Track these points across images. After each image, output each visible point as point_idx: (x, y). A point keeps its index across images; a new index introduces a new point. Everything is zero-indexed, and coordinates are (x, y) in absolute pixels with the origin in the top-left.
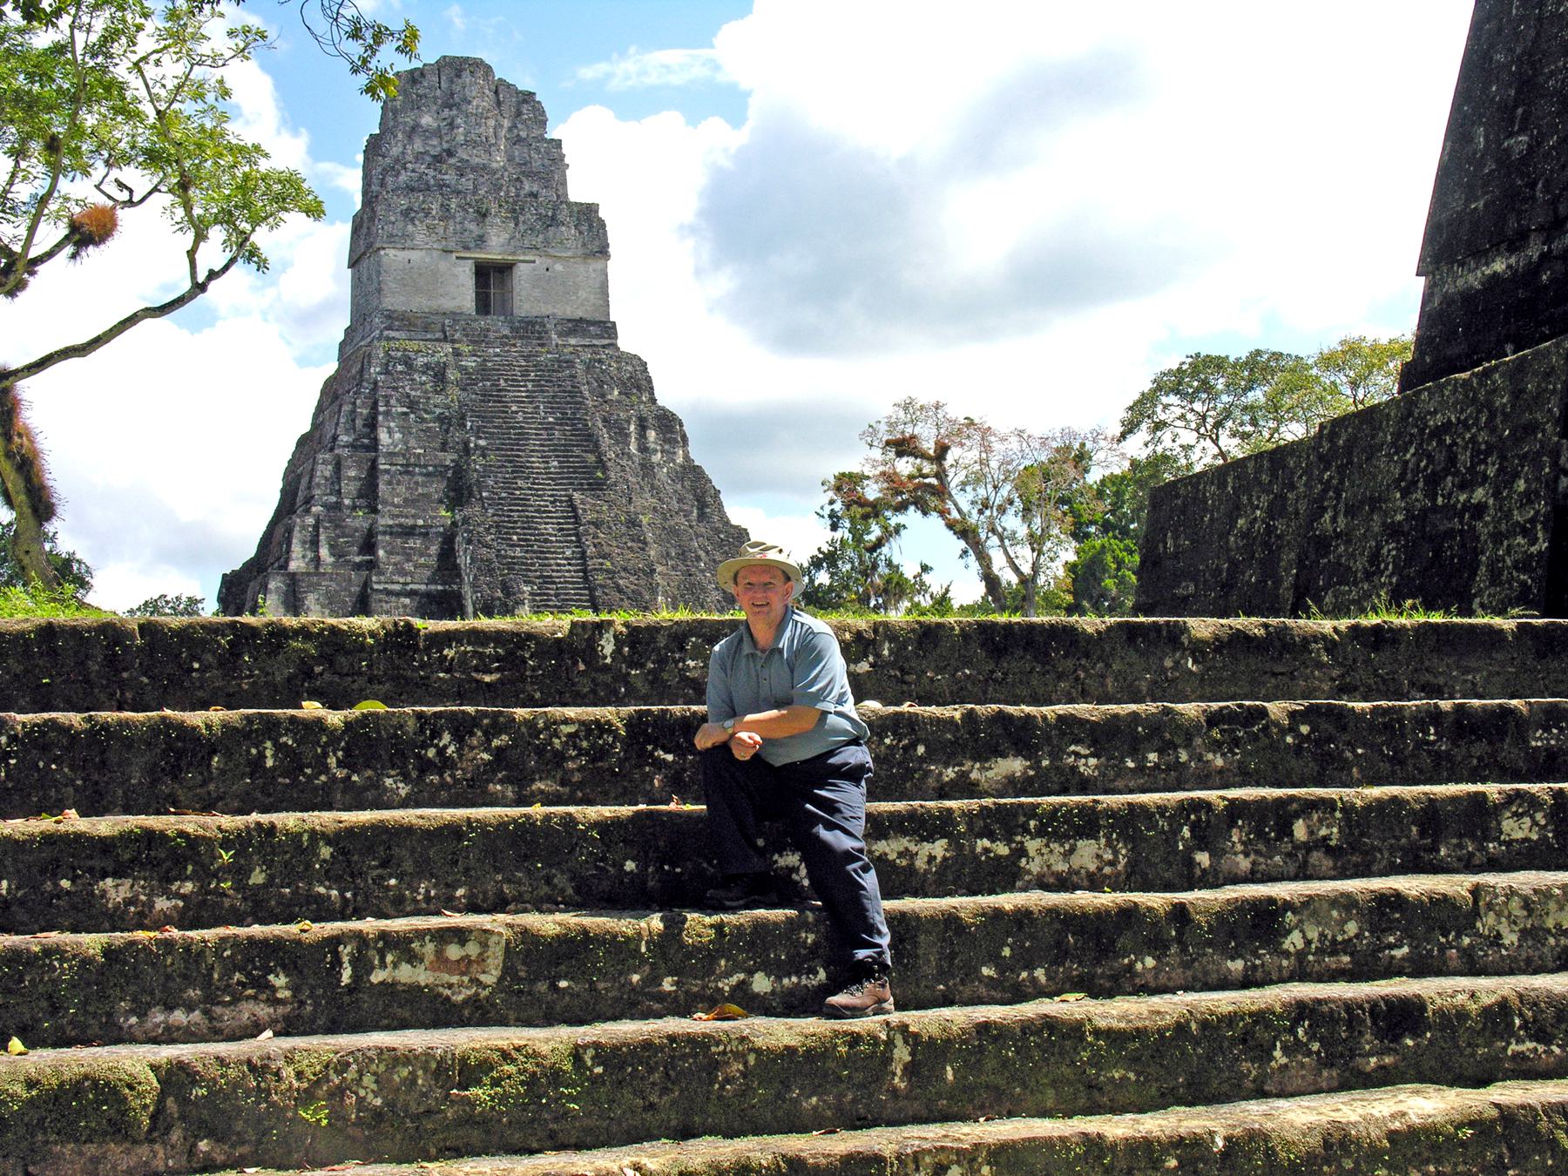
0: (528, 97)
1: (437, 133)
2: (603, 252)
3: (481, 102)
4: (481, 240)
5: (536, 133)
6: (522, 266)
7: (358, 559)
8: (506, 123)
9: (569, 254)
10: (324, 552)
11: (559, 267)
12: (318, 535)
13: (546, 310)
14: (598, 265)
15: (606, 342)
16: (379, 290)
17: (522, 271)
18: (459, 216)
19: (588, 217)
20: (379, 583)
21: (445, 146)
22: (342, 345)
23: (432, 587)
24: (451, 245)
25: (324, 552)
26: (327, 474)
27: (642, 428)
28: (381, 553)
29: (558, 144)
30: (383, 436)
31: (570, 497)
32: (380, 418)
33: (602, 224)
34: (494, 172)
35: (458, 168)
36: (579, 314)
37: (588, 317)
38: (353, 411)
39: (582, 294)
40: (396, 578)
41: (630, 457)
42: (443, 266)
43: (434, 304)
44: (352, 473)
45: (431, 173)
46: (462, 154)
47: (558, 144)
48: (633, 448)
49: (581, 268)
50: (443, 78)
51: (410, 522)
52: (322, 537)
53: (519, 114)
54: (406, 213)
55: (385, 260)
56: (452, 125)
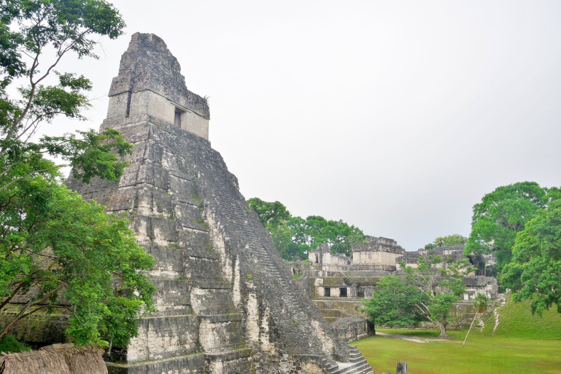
5: (178, 72)
6: (188, 113)
10: (155, 209)
11: (197, 117)
13: (192, 131)
14: (206, 121)
16: (147, 106)
23: (201, 231)
24: (170, 98)
25: (155, 209)
26: (149, 174)
29: (184, 78)
36: (201, 136)
40: (190, 226)
49: (202, 119)
52: (154, 203)
54: (158, 80)
55: (150, 95)
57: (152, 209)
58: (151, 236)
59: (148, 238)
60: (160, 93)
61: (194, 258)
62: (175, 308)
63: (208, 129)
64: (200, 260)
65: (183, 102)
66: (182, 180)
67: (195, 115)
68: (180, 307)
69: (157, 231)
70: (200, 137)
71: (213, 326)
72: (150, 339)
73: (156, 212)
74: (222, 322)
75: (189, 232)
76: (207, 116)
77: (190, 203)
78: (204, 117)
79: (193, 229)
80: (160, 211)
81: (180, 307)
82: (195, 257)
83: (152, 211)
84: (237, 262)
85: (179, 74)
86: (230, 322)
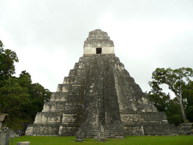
0: (106, 32)
1: (93, 37)
2: (113, 46)
10: (68, 82)
11: (107, 48)
14: (113, 47)
17: (102, 49)
18: (94, 43)
24: (93, 46)
25: (68, 82)
27: (117, 64)
29: (109, 37)
30: (80, 67)
33: (113, 42)
36: (110, 53)
41: (115, 68)
43: (91, 53)
44: (74, 72)
47: (109, 37)
48: (116, 67)
52: (68, 80)
59: (60, 90)
60: (89, 46)
62: (59, 110)
63: (113, 50)
65: (99, 45)
66: (83, 71)
68: (62, 110)
69: (63, 88)
71: (66, 115)
72: (43, 118)
73: (68, 83)
74: (71, 114)
75: (75, 86)
78: (111, 46)
80: (69, 81)
81: (62, 110)
85: (107, 36)
86: (76, 114)
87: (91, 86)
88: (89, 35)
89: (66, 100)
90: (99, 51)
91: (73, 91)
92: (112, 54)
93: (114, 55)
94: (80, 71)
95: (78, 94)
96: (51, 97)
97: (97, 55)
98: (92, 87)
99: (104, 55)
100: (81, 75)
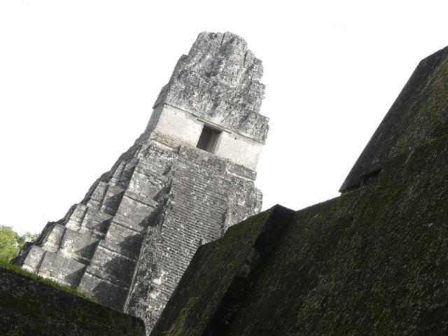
3: (236, 56)
4: (211, 115)
7: (97, 233)
8: (244, 70)
9: (248, 135)
12: (84, 216)
15: (250, 180)
17: (224, 135)
19: (263, 119)
20: (101, 246)
21: (213, 70)
22: (137, 140)
23: (125, 257)
25: (84, 224)
26: (100, 191)
28: (108, 234)
29: (264, 87)
30: (131, 185)
31: (201, 240)
32: (133, 176)
33: (268, 127)
34: (229, 89)
35: (214, 82)
36: (242, 163)
37: (246, 167)
38: (124, 169)
39: (247, 155)
40: (109, 247)
42: (190, 122)
43: (179, 135)
45: (202, 79)
46: (218, 76)
50: (225, 41)
51: (127, 225)
52: (86, 218)
53: (252, 67)
56: (220, 62)
57: (80, 224)
58: (60, 244)
60: (183, 108)
61: (91, 276)
63: (258, 155)
64: (99, 280)
65: (217, 121)
67: (238, 136)
69: (68, 243)
70: (236, 165)
73: (84, 229)
75: (104, 253)
76: (261, 138)
77: (131, 227)
79: (113, 251)
82: (93, 275)
83: (81, 225)
84: (134, 291)
85: (258, 83)
87: (157, 277)
88: (196, 47)
89: (69, 284)
90: (210, 135)
91: (97, 265)
92: (248, 170)
93: (252, 174)
94: (131, 201)
95: (111, 282)
96: (27, 259)
97: (198, 150)
98: (158, 281)
99: (220, 164)
100: (129, 216)
